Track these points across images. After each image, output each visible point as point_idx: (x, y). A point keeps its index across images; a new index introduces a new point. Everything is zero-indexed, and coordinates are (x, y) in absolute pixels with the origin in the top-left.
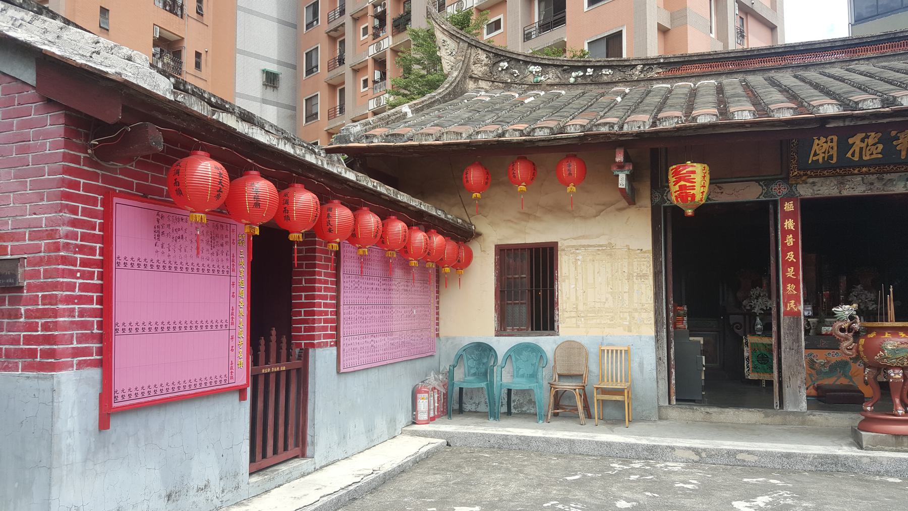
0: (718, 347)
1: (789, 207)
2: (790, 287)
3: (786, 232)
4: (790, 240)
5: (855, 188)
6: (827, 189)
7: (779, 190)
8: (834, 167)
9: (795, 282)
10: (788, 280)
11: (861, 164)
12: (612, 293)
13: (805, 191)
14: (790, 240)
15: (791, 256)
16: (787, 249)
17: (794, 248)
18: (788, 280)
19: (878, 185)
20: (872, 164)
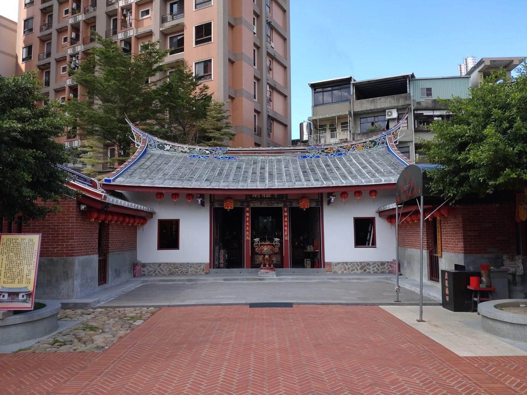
0: (230, 251)
1: (247, 209)
2: (247, 233)
3: (247, 217)
4: (248, 219)
5: (264, 205)
6: (258, 205)
7: (245, 204)
8: (259, 198)
9: (249, 231)
10: (247, 231)
11: (266, 198)
12: (196, 236)
13: (252, 205)
14: (248, 219)
15: (248, 224)
16: (247, 222)
17: (249, 221)
18: (247, 231)
19: (270, 204)
20: (268, 198)
